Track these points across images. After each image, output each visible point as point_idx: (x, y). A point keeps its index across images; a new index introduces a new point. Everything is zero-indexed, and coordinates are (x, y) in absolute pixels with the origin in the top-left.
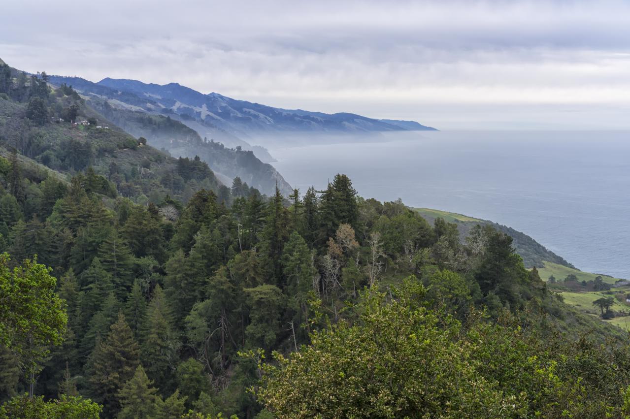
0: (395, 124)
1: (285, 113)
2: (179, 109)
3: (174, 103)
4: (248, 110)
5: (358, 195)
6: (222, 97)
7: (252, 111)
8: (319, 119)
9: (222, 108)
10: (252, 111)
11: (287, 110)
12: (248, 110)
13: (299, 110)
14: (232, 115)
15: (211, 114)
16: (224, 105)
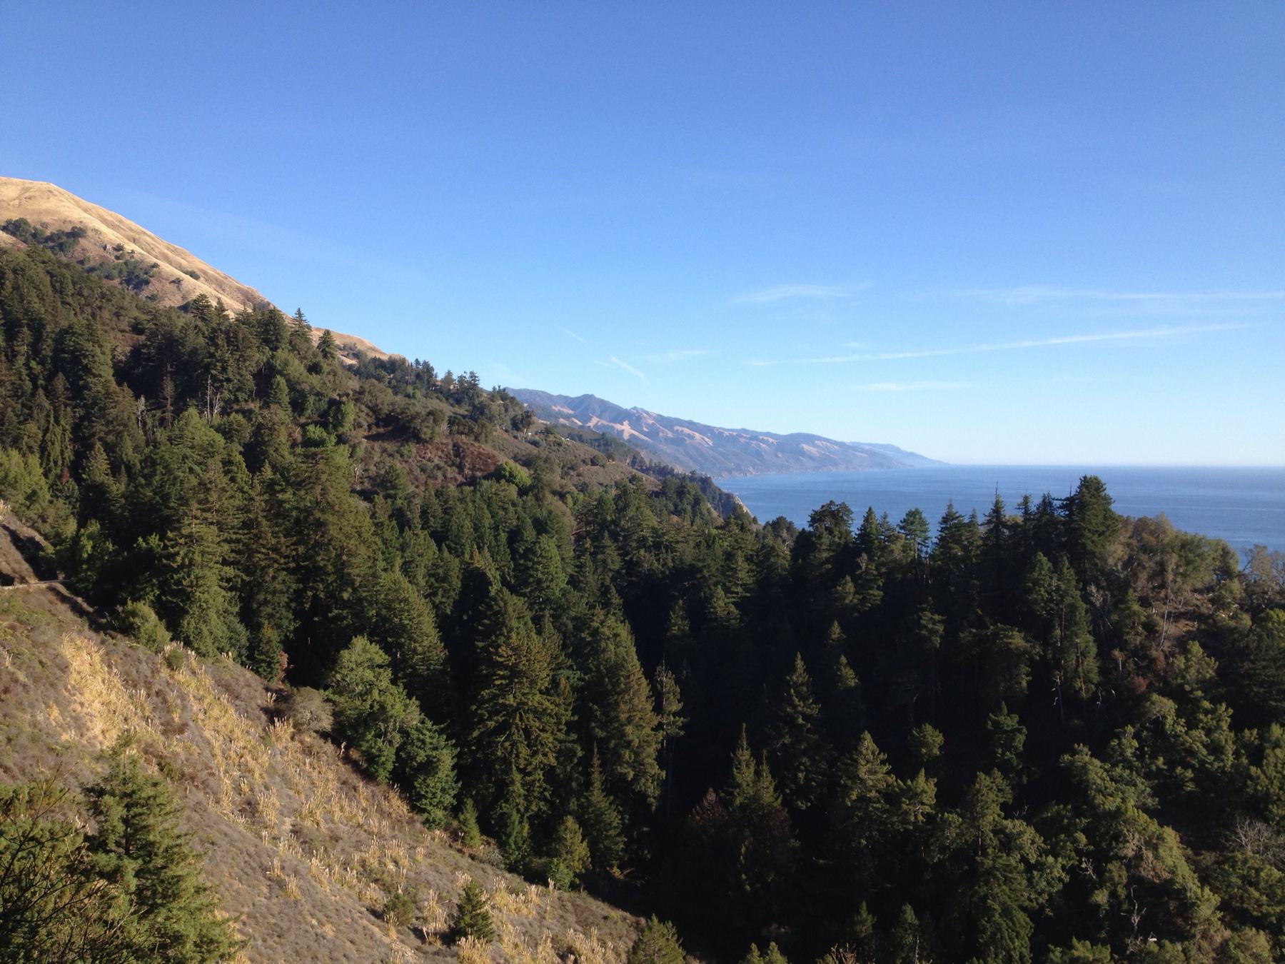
0: (867, 448)
1: (727, 433)
2: (596, 426)
3: (589, 419)
4: (680, 429)
5: (386, 403)
6: (647, 413)
7: (687, 431)
8: (771, 440)
9: (648, 426)
10: (687, 431)
11: (728, 430)
12: (680, 429)
13: (744, 430)
14: (661, 434)
15: (636, 433)
16: (651, 422)
